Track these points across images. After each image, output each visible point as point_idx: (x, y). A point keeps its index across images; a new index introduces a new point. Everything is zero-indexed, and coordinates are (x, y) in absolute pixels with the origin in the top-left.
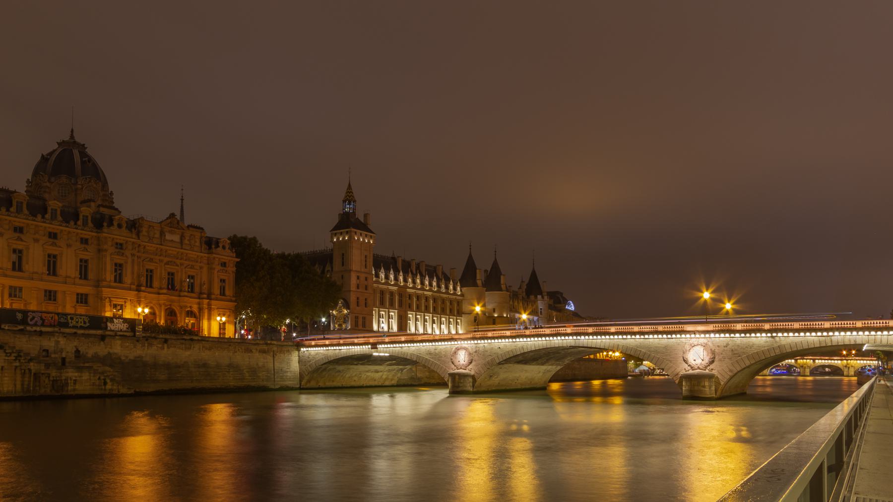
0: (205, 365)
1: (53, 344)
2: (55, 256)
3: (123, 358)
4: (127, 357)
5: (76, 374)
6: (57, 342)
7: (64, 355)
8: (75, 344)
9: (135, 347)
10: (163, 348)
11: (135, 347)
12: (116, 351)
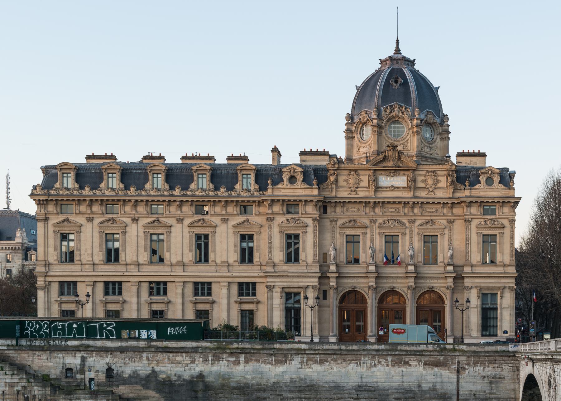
2: (206, 237)
3: (174, 378)
4: (179, 376)
8: (108, 360)
9: (193, 362)
10: (237, 363)
11: (193, 362)
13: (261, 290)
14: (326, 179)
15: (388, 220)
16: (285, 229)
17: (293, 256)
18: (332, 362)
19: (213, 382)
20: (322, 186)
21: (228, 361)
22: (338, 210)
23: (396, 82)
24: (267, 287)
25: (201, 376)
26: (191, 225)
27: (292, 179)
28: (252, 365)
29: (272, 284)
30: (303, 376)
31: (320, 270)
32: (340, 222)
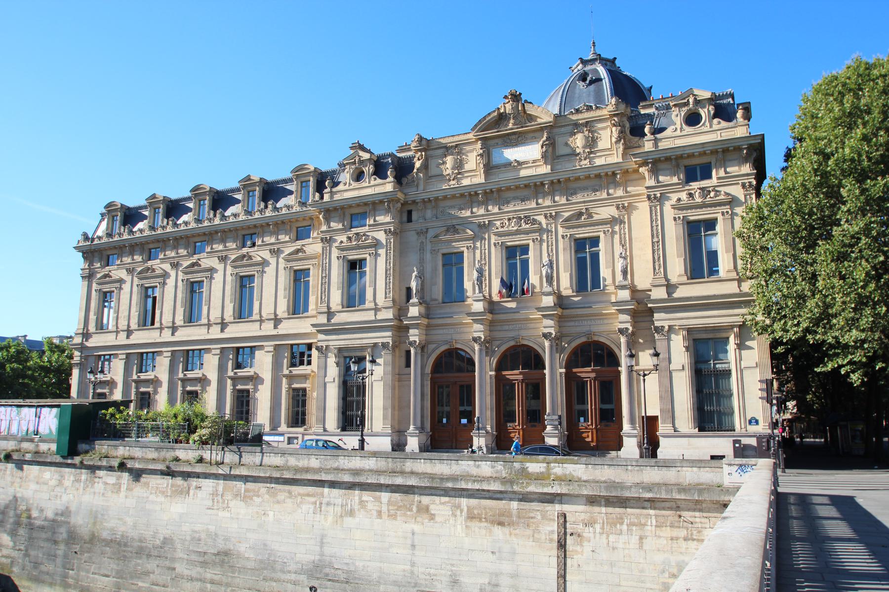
0: (224, 558)
3: (35, 514)
4: (42, 511)
10: (117, 487)
11: (60, 483)
15: (509, 219)
16: (345, 253)
18: (267, 496)
19: (80, 526)
20: (405, 181)
21: (106, 483)
22: (429, 213)
23: (584, 80)
25: (66, 512)
27: (359, 176)
29: (324, 344)
30: (212, 528)
32: (431, 233)
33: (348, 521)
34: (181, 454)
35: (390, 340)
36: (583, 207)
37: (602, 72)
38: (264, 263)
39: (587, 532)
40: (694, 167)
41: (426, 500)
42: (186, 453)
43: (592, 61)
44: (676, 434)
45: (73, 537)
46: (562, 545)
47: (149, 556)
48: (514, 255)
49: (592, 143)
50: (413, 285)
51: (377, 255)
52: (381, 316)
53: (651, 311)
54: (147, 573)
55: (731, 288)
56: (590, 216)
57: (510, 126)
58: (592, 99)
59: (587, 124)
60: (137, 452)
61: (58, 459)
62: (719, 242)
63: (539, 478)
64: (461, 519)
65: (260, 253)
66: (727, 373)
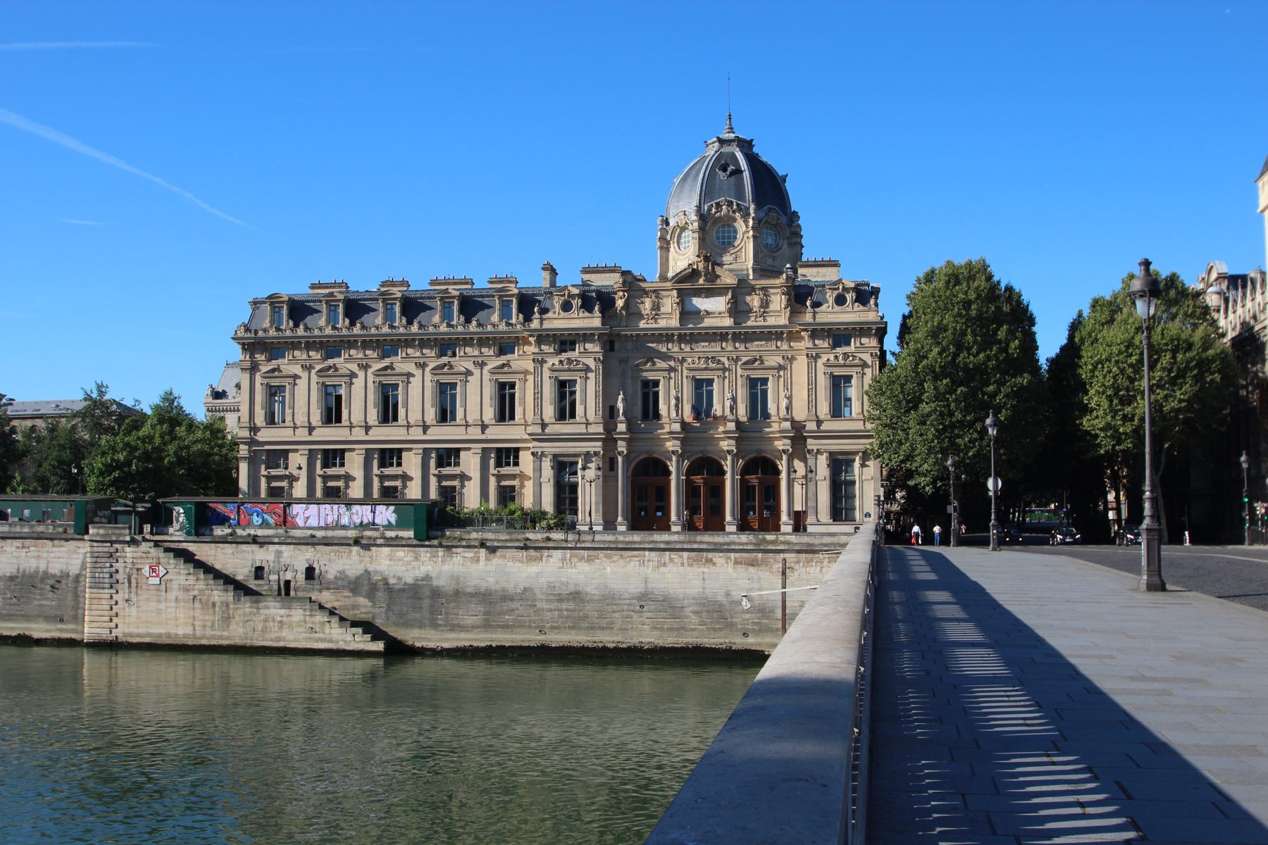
1: (271, 557)
3: (392, 581)
4: (400, 579)
5: (283, 611)
6: (279, 554)
7: (289, 576)
9: (416, 559)
12: (378, 568)
13: (526, 459)
14: (613, 302)
16: (556, 374)
17: (566, 411)
20: (607, 314)
22: (630, 346)
23: (725, 170)
24: (533, 454)
25: (427, 578)
26: (378, 374)
27: (566, 307)
28: (497, 561)
29: (539, 451)
31: (605, 429)
33: (663, 569)
34: (531, 536)
35: (600, 450)
36: (757, 355)
37: (739, 156)
38: (469, 373)
39: (796, 567)
40: (839, 336)
41: (710, 555)
42: (535, 536)
43: (729, 142)
44: (818, 523)
45: (436, 593)
46: (784, 573)
47: (512, 600)
48: (702, 388)
49: (765, 304)
50: (620, 405)
51: (587, 378)
52: (592, 429)
53: (805, 438)
54: (513, 610)
55: (859, 426)
56: (762, 362)
57: (701, 281)
58: (732, 193)
59: (762, 289)
60: (490, 536)
61: (415, 542)
62: (853, 392)
63: (772, 542)
64: (731, 564)
65: (463, 364)
66: (854, 482)
